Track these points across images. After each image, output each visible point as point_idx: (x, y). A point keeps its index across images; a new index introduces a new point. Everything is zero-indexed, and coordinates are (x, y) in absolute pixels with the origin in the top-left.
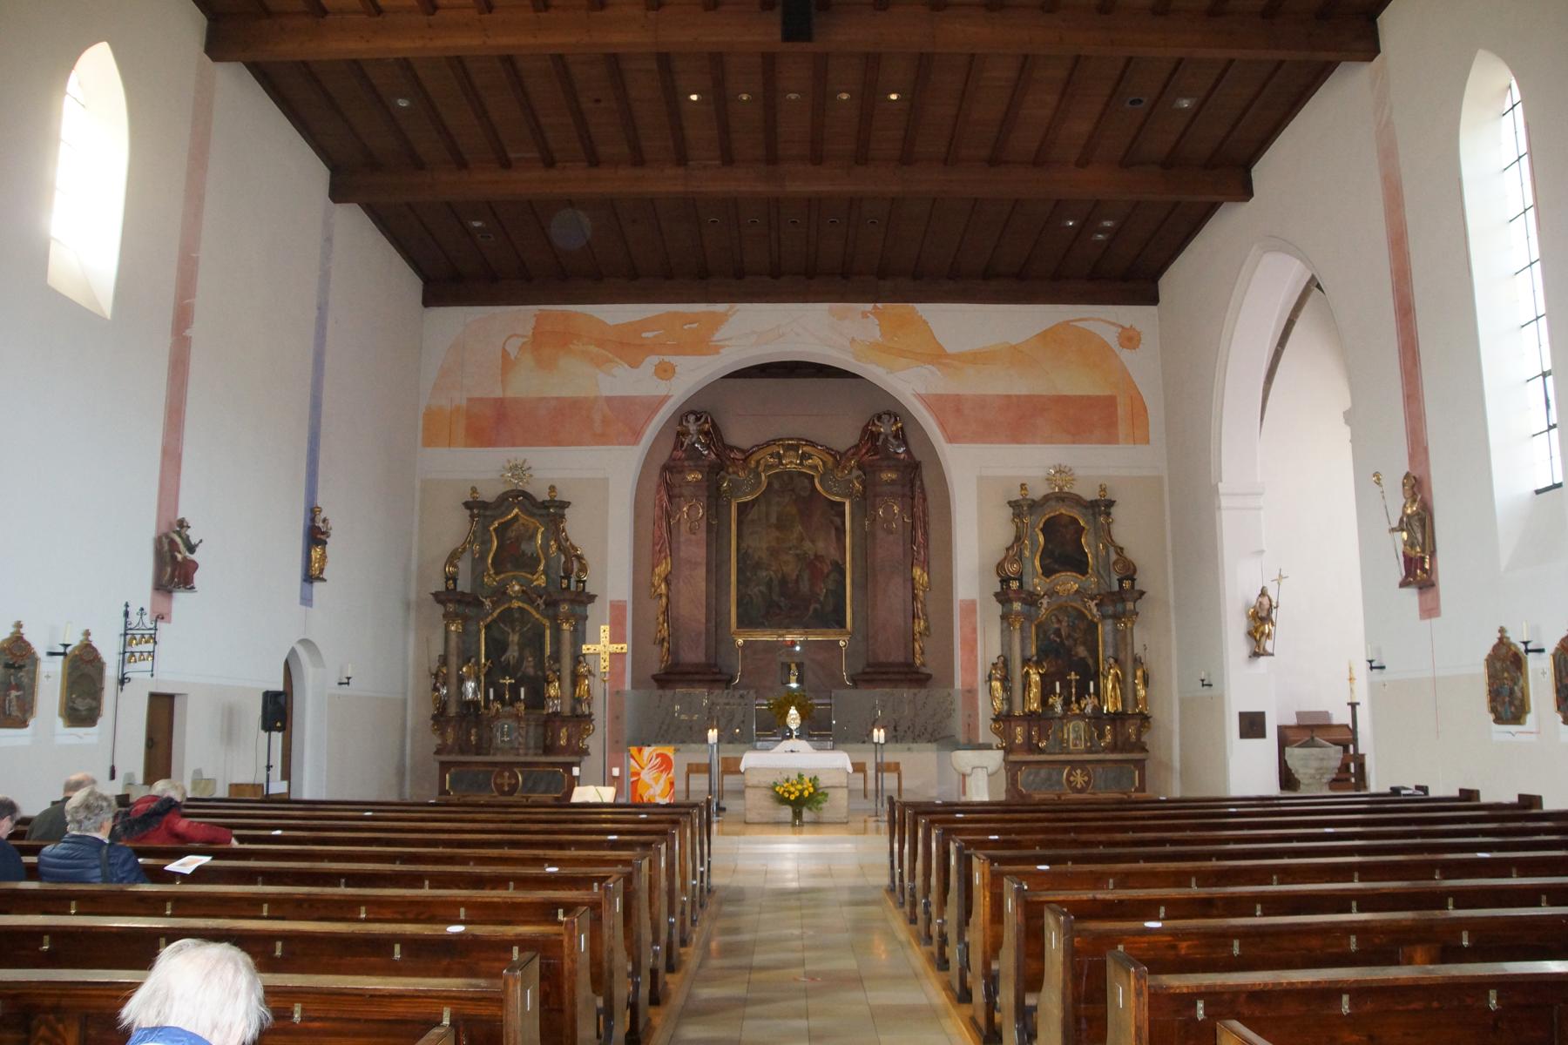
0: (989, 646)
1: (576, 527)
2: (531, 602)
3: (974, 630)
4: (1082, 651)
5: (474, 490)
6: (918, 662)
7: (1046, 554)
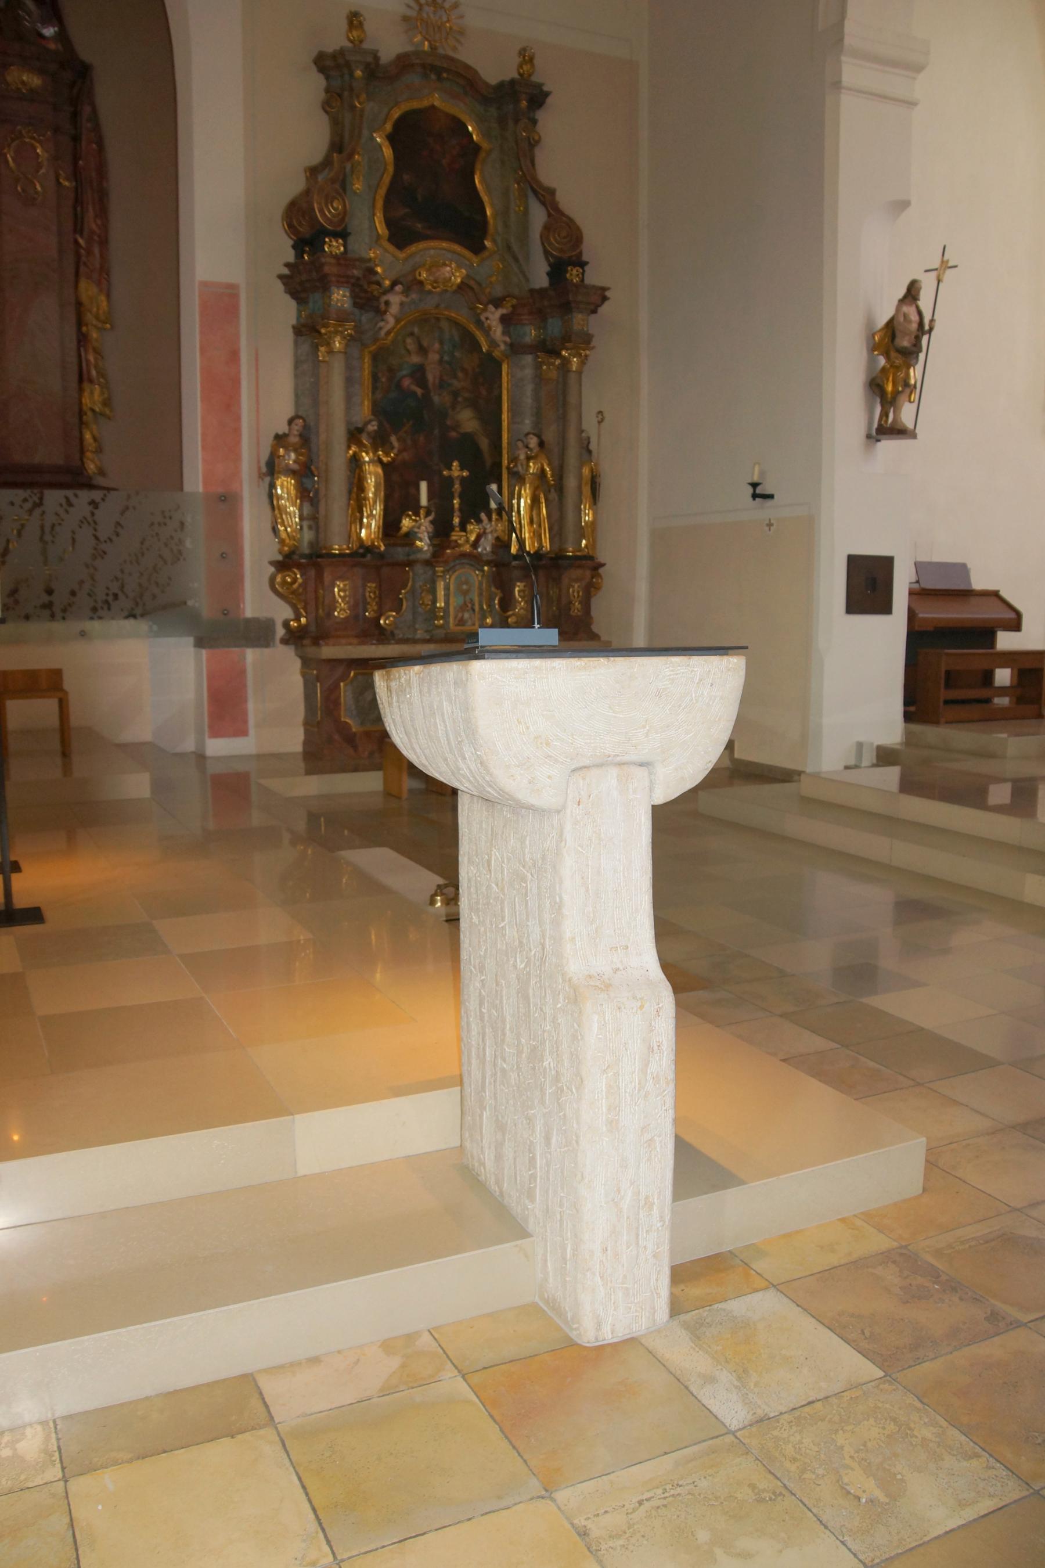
0: (268, 397)
3: (234, 356)
4: (467, 420)
6: (91, 467)
7: (397, 195)
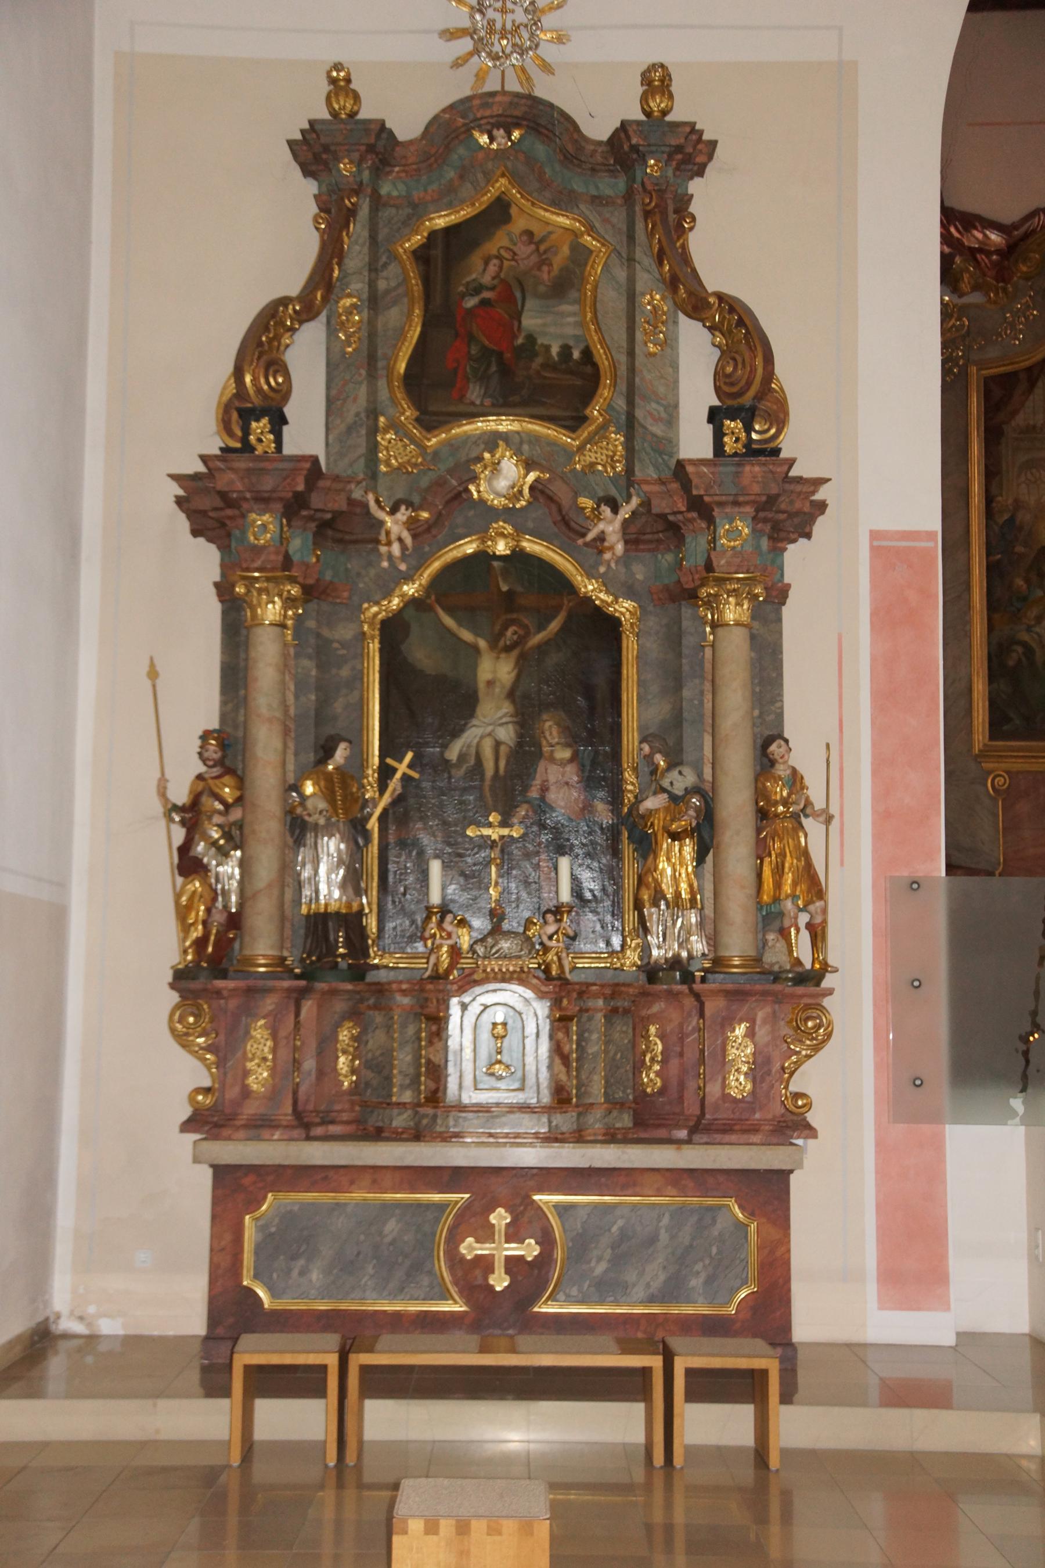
1: (728, 238)
2: (567, 528)
5: (340, 85)
